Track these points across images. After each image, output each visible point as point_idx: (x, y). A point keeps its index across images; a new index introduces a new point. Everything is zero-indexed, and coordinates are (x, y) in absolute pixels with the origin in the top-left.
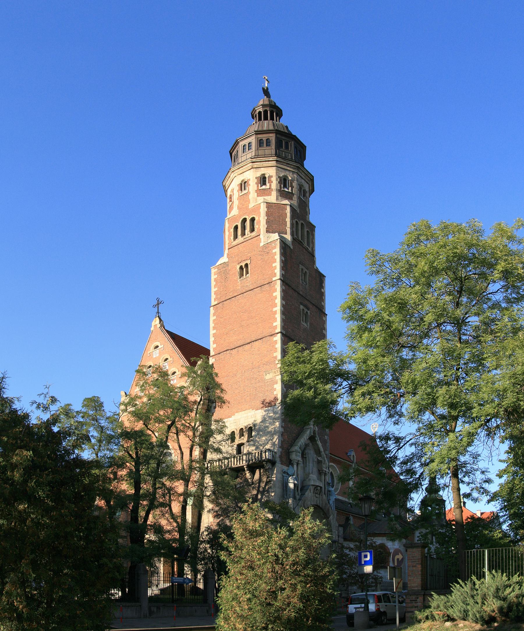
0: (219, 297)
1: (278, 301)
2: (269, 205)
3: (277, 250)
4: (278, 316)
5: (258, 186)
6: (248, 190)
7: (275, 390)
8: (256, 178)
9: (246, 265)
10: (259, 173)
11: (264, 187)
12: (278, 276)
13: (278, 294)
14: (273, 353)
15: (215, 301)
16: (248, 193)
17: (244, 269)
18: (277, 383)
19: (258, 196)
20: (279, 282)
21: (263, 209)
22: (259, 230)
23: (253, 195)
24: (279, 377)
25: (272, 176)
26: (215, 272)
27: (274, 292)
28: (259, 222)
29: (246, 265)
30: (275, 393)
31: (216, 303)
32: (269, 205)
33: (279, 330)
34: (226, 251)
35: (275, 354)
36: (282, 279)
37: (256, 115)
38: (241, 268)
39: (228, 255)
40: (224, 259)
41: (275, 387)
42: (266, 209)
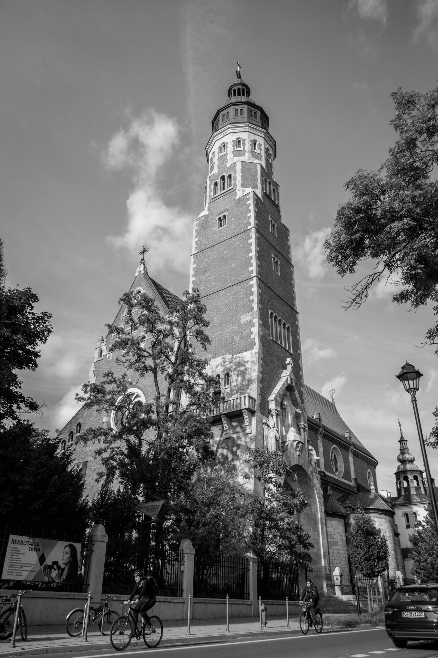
0: (199, 246)
1: (253, 247)
2: (243, 163)
3: (251, 202)
4: (254, 262)
5: (234, 148)
6: (227, 151)
7: (252, 333)
8: (233, 141)
9: (224, 217)
10: (235, 138)
11: (239, 149)
12: (253, 225)
13: (253, 241)
14: (249, 296)
15: (195, 250)
16: (226, 154)
17: (222, 221)
18: (253, 326)
19: (234, 156)
20: (253, 230)
21: (239, 167)
22: (235, 185)
23: (230, 156)
24: (256, 321)
25: (245, 140)
26: (196, 224)
27: (249, 239)
28: (235, 178)
29: (224, 217)
30: (252, 336)
31: (196, 252)
32: (243, 163)
33: (254, 274)
34: (207, 205)
35: (251, 298)
36: (256, 227)
37: (232, 93)
38: (220, 219)
39: (209, 208)
40: (205, 212)
41: (252, 331)
42: (241, 167)
